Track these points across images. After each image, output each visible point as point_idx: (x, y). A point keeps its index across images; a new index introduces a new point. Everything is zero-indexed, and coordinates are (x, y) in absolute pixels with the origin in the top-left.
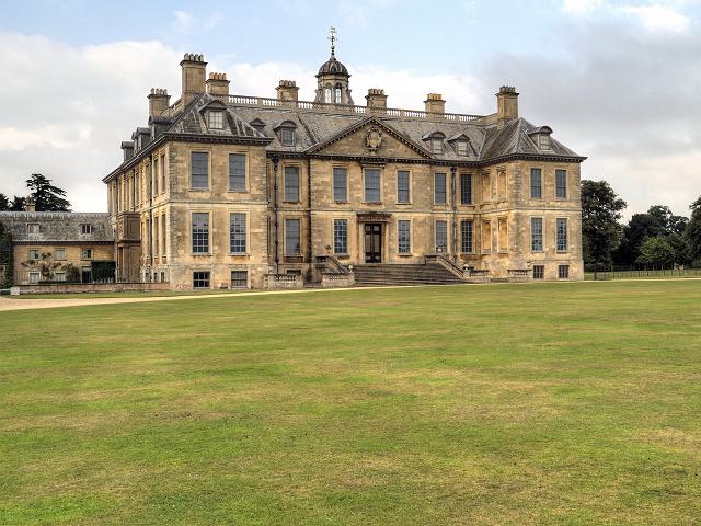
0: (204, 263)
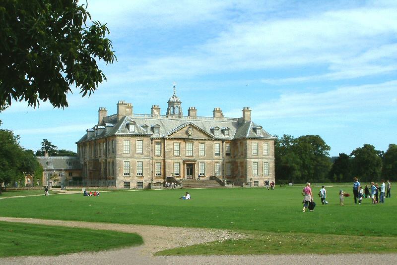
0: (128, 180)
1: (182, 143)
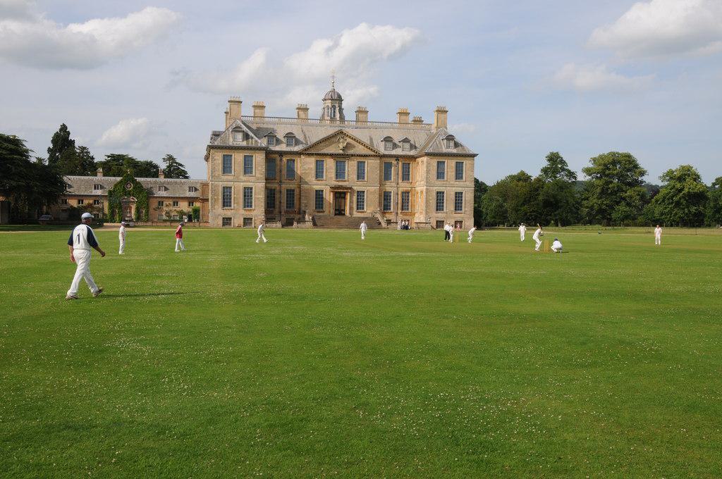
0: (228, 213)
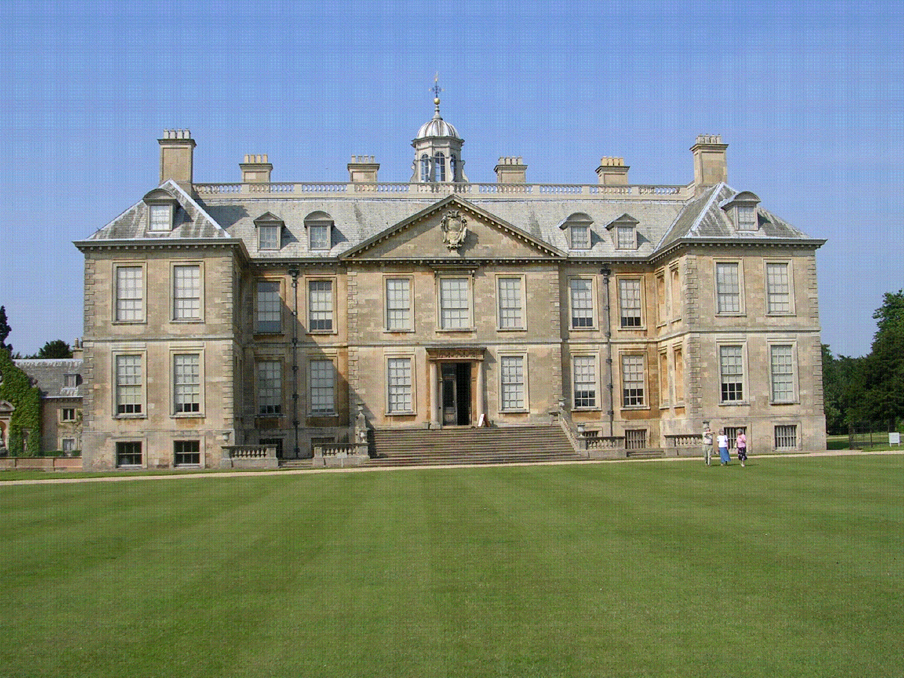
0: (132, 431)
1: (424, 280)
